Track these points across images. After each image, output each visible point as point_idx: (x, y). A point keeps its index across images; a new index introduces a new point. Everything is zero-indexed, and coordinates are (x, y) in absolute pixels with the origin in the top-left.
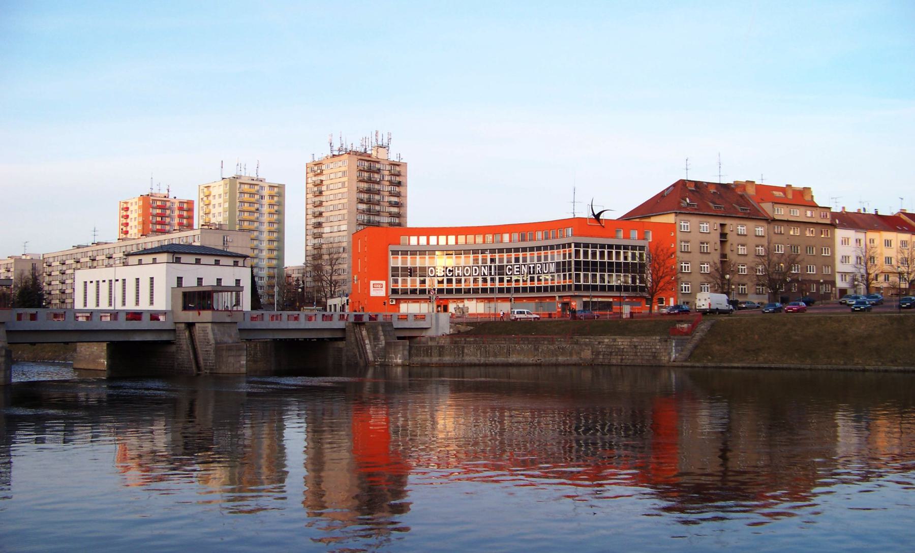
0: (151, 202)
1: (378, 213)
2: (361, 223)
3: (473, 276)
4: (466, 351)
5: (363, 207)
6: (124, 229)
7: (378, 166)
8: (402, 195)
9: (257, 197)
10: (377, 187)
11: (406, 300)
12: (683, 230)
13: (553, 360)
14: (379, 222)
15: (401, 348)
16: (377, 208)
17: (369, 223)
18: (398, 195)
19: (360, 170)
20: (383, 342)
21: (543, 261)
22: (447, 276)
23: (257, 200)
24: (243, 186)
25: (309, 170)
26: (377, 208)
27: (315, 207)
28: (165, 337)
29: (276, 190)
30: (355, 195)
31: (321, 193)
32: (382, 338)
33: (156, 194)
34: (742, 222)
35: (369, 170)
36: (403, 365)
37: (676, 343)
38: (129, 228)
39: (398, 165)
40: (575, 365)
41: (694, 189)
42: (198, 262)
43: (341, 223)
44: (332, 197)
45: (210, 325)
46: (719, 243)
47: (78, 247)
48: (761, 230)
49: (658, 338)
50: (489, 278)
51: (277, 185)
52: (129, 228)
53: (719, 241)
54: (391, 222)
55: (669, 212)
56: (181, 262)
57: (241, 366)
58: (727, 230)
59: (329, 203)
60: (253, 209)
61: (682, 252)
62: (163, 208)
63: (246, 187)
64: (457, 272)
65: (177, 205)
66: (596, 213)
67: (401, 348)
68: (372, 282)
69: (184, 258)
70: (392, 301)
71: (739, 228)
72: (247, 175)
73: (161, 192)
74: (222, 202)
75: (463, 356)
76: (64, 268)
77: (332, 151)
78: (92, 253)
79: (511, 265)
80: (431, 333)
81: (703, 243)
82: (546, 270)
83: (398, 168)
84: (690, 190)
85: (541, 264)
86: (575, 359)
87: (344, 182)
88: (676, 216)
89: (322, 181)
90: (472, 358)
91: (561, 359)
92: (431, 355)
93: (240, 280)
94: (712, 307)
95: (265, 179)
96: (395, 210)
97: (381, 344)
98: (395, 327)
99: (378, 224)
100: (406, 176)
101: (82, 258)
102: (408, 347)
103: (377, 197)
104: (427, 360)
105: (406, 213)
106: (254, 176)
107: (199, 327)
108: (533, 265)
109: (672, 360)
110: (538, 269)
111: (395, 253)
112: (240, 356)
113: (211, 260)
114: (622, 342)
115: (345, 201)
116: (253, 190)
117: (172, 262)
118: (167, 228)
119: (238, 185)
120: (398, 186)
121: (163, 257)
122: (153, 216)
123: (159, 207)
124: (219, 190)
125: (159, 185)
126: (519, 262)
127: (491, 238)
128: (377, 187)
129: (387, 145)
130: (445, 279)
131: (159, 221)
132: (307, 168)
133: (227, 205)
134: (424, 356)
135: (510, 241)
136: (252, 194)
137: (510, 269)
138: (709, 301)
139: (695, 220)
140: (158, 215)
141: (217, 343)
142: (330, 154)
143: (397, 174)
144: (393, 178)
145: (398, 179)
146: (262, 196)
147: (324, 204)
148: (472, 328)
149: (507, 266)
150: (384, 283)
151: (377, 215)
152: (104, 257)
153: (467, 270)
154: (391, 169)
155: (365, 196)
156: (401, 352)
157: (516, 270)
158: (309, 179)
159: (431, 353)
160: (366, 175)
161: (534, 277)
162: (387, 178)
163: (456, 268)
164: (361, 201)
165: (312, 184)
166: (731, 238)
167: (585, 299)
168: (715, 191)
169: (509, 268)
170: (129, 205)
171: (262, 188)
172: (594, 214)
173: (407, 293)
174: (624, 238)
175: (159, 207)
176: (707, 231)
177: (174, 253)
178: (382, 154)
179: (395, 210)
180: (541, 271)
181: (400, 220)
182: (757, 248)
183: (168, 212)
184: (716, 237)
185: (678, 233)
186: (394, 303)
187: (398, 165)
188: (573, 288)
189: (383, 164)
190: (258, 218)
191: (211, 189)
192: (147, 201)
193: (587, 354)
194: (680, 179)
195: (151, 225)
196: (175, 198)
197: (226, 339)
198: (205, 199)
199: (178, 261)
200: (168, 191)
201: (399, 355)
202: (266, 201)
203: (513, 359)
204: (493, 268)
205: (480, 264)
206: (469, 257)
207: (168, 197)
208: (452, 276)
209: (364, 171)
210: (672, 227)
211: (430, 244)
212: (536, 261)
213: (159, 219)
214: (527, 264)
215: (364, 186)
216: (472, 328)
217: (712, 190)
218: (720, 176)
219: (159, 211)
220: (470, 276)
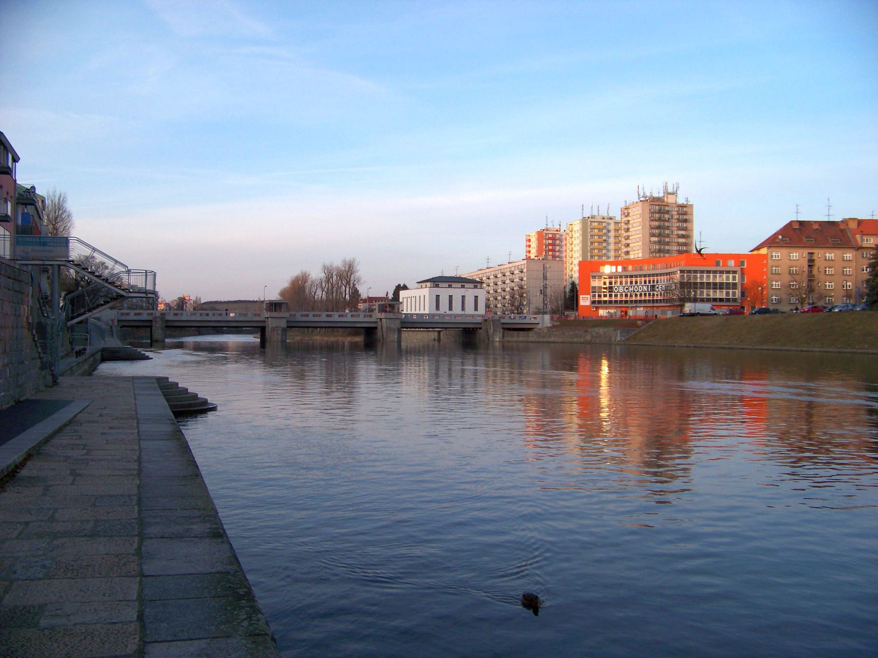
0: (544, 235)
1: (668, 244)
2: (653, 251)
5: (655, 239)
7: (667, 208)
8: (689, 229)
9: (604, 231)
10: (667, 224)
11: (603, 308)
12: (774, 259)
13: (571, 340)
14: (668, 250)
15: (498, 332)
16: (667, 240)
17: (660, 251)
19: (651, 212)
20: (492, 330)
22: (625, 292)
23: (605, 234)
24: (593, 224)
25: (622, 212)
26: (667, 240)
27: (626, 240)
28: (373, 325)
30: (647, 231)
32: (492, 328)
33: (550, 228)
34: (830, 250)
35: (660, 212)
36: (499, 342)
37: (621, 332)
39: (685, 207)
40: (581, 343)
41: (798, 227)
42: (450, 286)
46: (807, 266)
48: (849, 255)
49: (613, 328)
50: (647, 293)
53: (807, 266)
54: (679, 250)
58: (815, 257)
60: (600, 240)
61: (772, 274)
62: (553, 239)
63: (596, 224)
64: (630, 289)
66: (699, 250)
68: (581, 296)
69: (441, 285)
70: (593, 309)
71: (827, 255)
77: (639, 198)
80: (540, 326)
81: (793, 267)
83: (685, 209)
84: (794, 229)
86: (582, 340)
89: (629, 221)
91: (575, 340)
93: (477, 296)
94: (691, 312)
95: (615, 217)
98: (502, 322)
99: (668, 251)
100: (692, 215)
102: (502, 332)
103: (667, 232)
104: (511, 339)
106: (605, 214)
109: (617, 340)
111: (594, 277)
113: (459, 285)
114: (601, 330)
115: (640, 236)
116: (601, 227)
119: (589, 223)
121: (429, 284)
123: (550, 239)
124: (577, 227)
125: (552, 222)
127: (651, 266)
128: (667, 224)
130: (624, 294)
131: (550, 249)
132: (621, 211)
133: (581, 238)
135: (648, 270)
136: (600, 230)
137: (658, 288)
138: (690, 308)
139: (785, 251)
140: (550, 244)
141: (387, 328)
142: (636, 199)
143: (684, 214)
145: (685, 217)
150: (589, 296)
151: (668, 245)
153: (636, 288)
154: (679, 210)
155: (657, 231)
157: (660, 288)
160: (657, 215)
161: (612, 294)
162: (675, 217)
164: (653, 235)
166: (818, 263)
168: (818, 228)
170: (531, 238)
171: (609, 224)
172: (697, 251)
173: (596, 303)
174: (723, 265)
175: (550, 239)
176: (796, 258)
177: (434, 282)
178: (670, 200)
182: (845, 269)
183: (558, 242)
184: (805, 264)
185: (769, 261)
186: (595, 309)
187: (685, 207)
189: (672, 207)
190: (605, 247)
191: (573, 226)
193: (588, 338)
194: (790, 221)
196: (565, 231)
197: (392, 326)
199: (437, 286)
203: (552, 339)
204: (649, 286)
205: (643, 284)
207: (560, 231)
208: (628, 292)
209: (656, 213)
210: (765, 257)
213: (550, 247)
215: (657, 223)
217: (816, 227)
219: (550, 242)
220: (618, 292)
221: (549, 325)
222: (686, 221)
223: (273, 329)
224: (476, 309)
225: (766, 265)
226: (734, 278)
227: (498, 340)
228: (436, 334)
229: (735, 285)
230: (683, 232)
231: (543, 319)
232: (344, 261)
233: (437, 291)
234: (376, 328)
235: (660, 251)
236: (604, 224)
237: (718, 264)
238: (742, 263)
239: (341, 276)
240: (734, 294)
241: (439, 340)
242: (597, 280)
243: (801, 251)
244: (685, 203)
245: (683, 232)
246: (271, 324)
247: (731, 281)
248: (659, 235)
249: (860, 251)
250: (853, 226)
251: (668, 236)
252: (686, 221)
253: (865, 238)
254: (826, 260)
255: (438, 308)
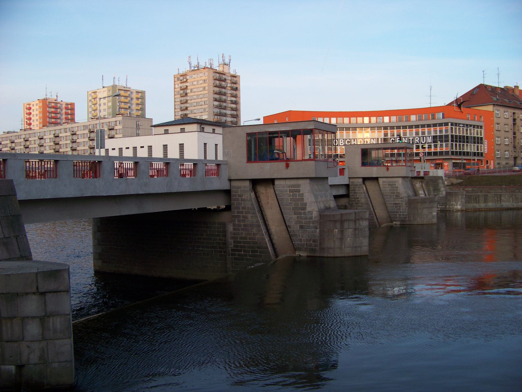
0: (48, 103)
1: (225, 108)
3: (340, 146)
4: (503, 198)
5: (216, 103)
6: (28, 122)
15: (460, 197)
18: (236, 96)
21: (420, 135)
24: (120, 91)
25: (176, 79)
27: (182, 104)
29: (140, 94)
30: (212, 96)
31: (186, 94)
36: (462, 211)
38: (31, 121)
43: (203, 114)
44: (195, 97)
45: (400, 180)
46: (512, 125)
47: (8, 133)
51: (141, 91)
52: (31, 121)
55: (489, 104)
56: (205, 131)
57: (433, 217)
58: (516, 116)
59: (193, 101)
60: (127, 107)
65: (64, 106)
67: (460, 197)
72: (120, 85)
73: (52, 97)
74: (107, 102)
75: (500, 202)
76: (13, 145)
77: (190, 67)
78: (25, 136)
79: (394, 138)
82: (423, 141)
85: (419, 137)
87: (205, 87)
88: (493, 107)
89: (187, 86)
90: (507, 203)
92: (479, 202)
96: (234, 106)
97: (442, 194)
100: (239, 84)
101: (16, 139)
104: (477, 206)
107: (384, 182)
108: (412, 138)
110: (416, 140)
112: (432, 208)
116: (127, 95)
117: (200, 131)
118: (59, 121)
120: (235, 91)
122: (49, 113)
123: (53, 107)
126: (425, 135)
129: (229, 63)
132: (175, 78)
133: (110, 104)
134: (474, 203)
136: (126, 97)
144: (233, 85)
145: (235, 86)
146: (132, 99)
147: (189, 101)
148: (462, 181)
149: (390, 138)
152: (37, 138)
155: (217, 96)
156: (460, 200)
158: (177, 86)
159: (479, 200)
162: (229, 85)
163: (353, 140)
164: (216, 100)
165: (179, 88)
167: (454, 161)
169: (392, 140)
170: (31, 106)
175: (53, 107)
179: (234, 106)
180: (419, 142)
181: (236, 113)
184: (511, 121)
185: (495, 118)
188: (450, 153)
189: (227, 76)
191: (97, 93)
192: (45, 103)
195: (48, 119)
198: (93, 100)
200: (57, 97)
201: (459, 203)
202: (135, 101)
206: (381, 132)
211: (364, 123)
212: (414, 135)
214: (407, 137)
215: (217, 89)
216: (462, 181)
218: (499, 82)
219: (53, 110)
242: (351, 132)
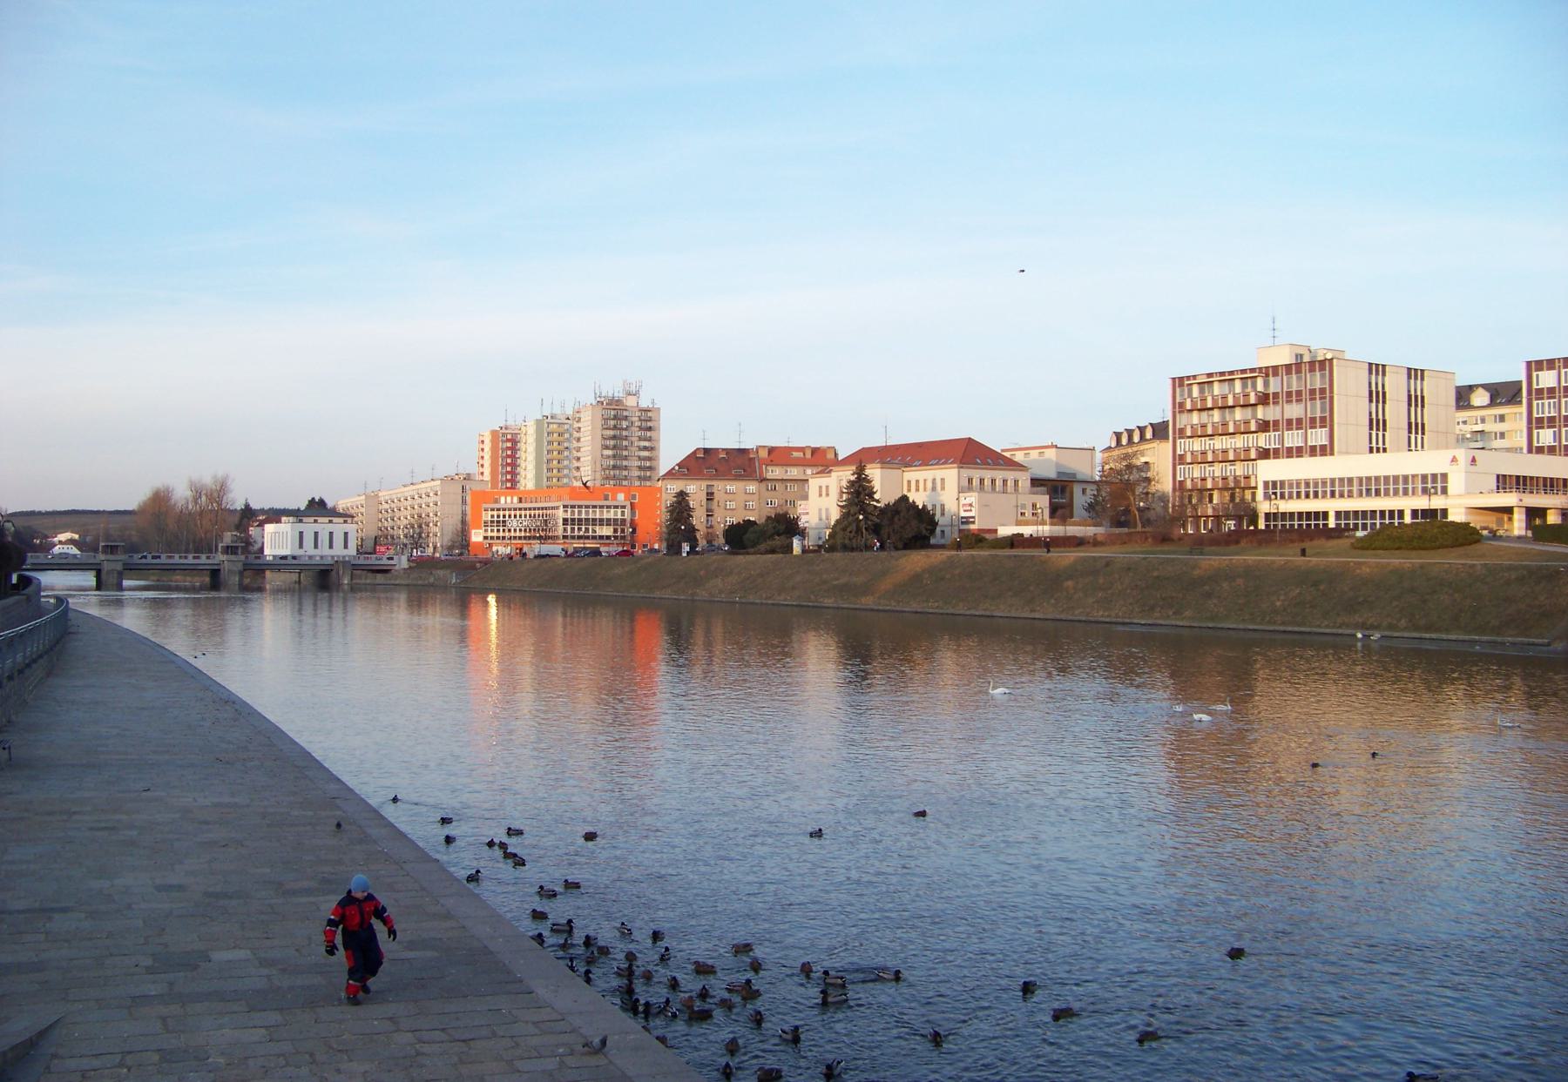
1: (626, 458)
5: (610, 452)
7: (625, 413)
10: (624, 433)
16: (625, 453)
24: (551, 426)
26: (625, 453)
28: (216, 567)
35: (615, 418)
48: (752, 487)
58: (715, 490)
63: (555, 426)
68: (473, 531)
80: (397, 568)
83: (649, 414)
89: (580, 428)
91: (420, 582)
96: (645, 454)
103: (625, 443)
105: (658, 457)
116: (561, 430)
123: (508, 440)
140: (508, 448)
143: (648, 422)
144: (644, 424)
155: (612, 443)
160: (612, 423)
164: (607, 448)
175: (508, 440)
178: (630, 402)
179: (645, 454)
185: (664, 494)
197: (235, 569)
199: (301, 521)
215: (611, 433)
219: (509, 445)
221: (406, 567)
222: (650, 429)
223: (109, 572)
224: (346, 547)
225: (659, 499)
226: (623, 513)
227: (346, 582)
228: (297, 575)
229: (623, 521)
230: (646, 444)
231: (400, 559)
232: (215, 477)
233: (301, 527)
234: (219, 570)
235: (615, 467)
236: (566, 427)
237: (606, 498)
238: (634, 497)
239: (210, 498)
240: (623, 531)
241: (299, 582)
243: (699, 483)
244: (651, 406)
245: (646, 444)
246: (106, 567)
247: (619, 517)
248: (615, 447)
249: (763, 485)
250: (764, 454)
251: (626, 448)
252: (650, 429)
253: (770, 468)
254: (726, 493)
255: (301, 546)
